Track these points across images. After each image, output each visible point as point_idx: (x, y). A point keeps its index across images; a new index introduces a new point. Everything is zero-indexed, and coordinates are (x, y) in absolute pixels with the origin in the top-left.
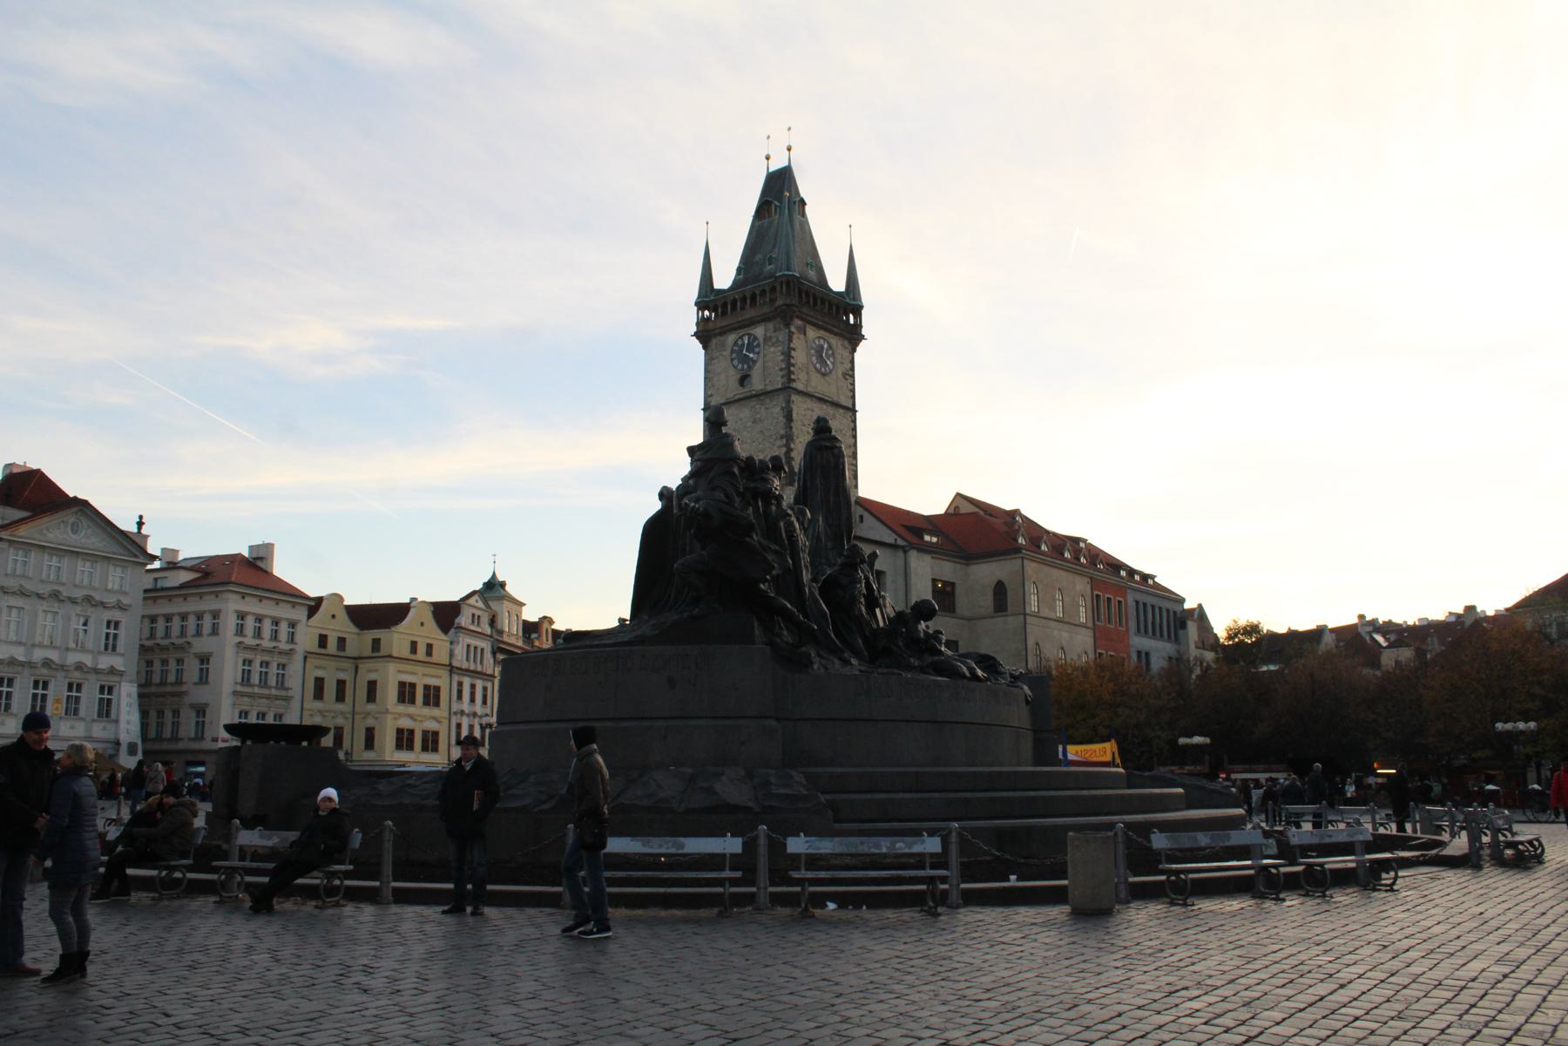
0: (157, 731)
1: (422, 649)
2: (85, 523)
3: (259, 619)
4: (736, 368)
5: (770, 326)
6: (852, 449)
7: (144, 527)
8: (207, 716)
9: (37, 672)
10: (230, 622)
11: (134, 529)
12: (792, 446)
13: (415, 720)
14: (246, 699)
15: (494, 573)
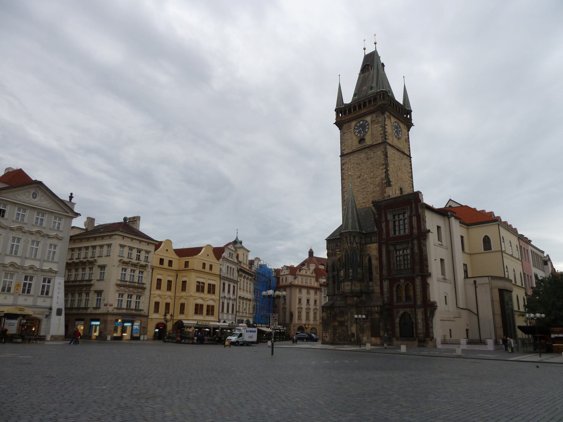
0: (85, 304)
1: (207, 267)
2: (40, 194)
3: (131, 248)
4: (357, 136)
5: (374, 115)
6: (411, 174)
7: (73, 199)
8: (102, 296)
9: (7, 269)
10: (116, 250)
11: (68, 199)
12: (388, 169)
13: (204, 300)
14: (122, 288)
15: (237, 237)
